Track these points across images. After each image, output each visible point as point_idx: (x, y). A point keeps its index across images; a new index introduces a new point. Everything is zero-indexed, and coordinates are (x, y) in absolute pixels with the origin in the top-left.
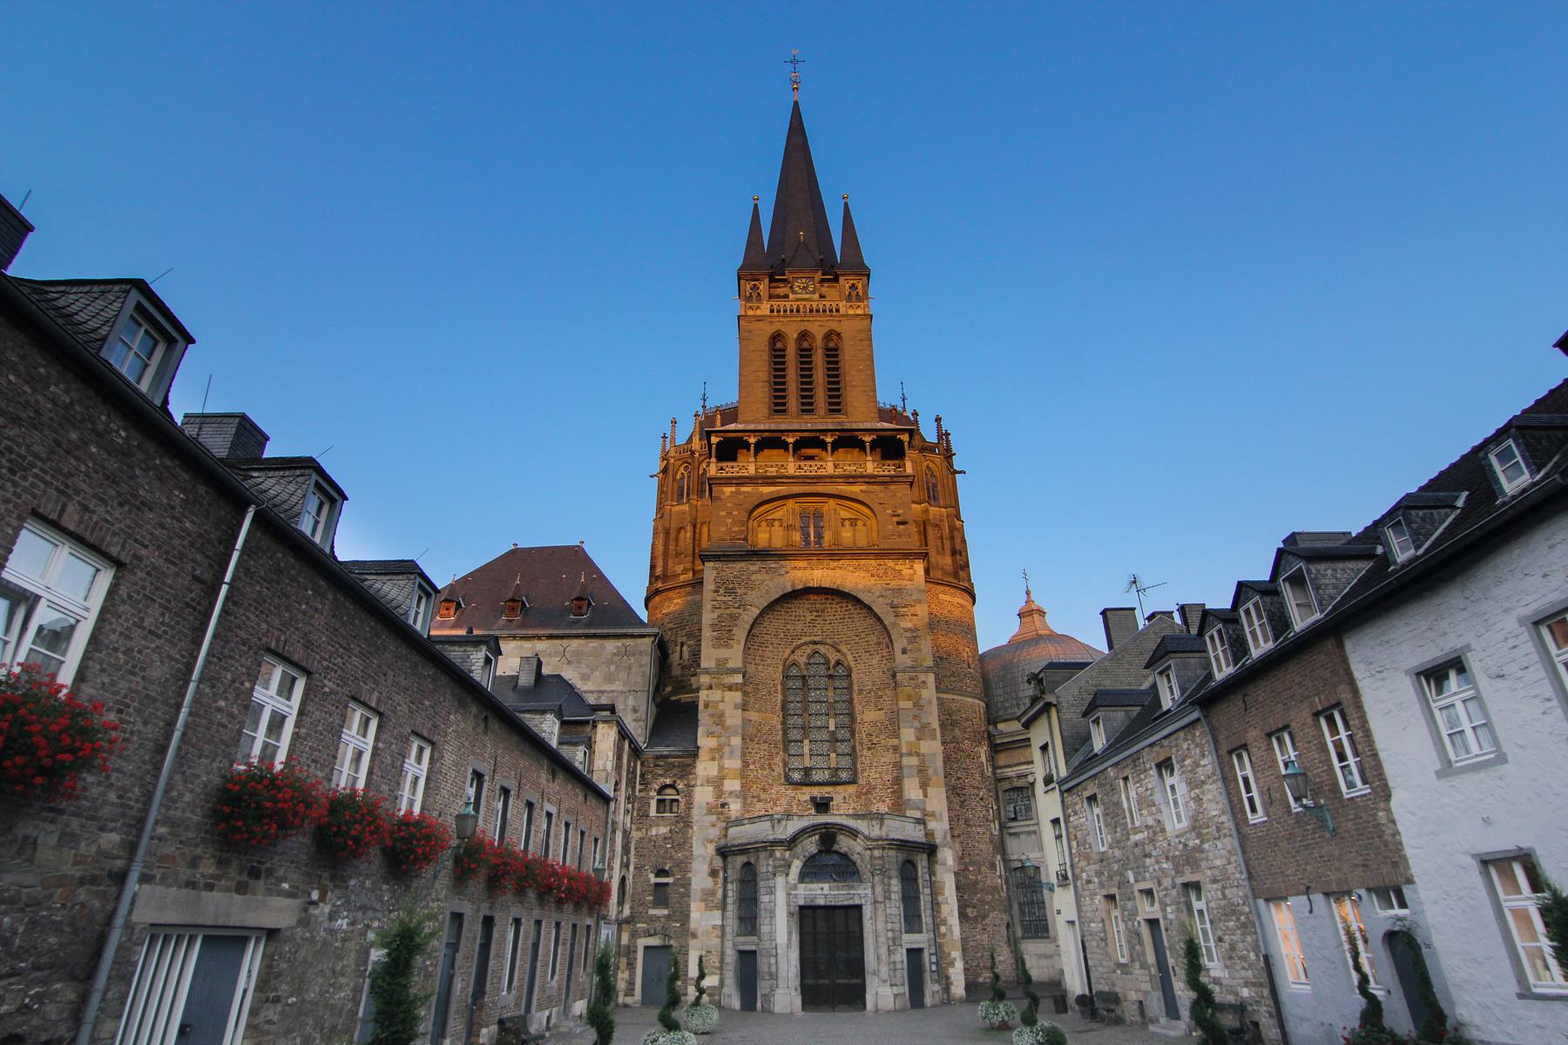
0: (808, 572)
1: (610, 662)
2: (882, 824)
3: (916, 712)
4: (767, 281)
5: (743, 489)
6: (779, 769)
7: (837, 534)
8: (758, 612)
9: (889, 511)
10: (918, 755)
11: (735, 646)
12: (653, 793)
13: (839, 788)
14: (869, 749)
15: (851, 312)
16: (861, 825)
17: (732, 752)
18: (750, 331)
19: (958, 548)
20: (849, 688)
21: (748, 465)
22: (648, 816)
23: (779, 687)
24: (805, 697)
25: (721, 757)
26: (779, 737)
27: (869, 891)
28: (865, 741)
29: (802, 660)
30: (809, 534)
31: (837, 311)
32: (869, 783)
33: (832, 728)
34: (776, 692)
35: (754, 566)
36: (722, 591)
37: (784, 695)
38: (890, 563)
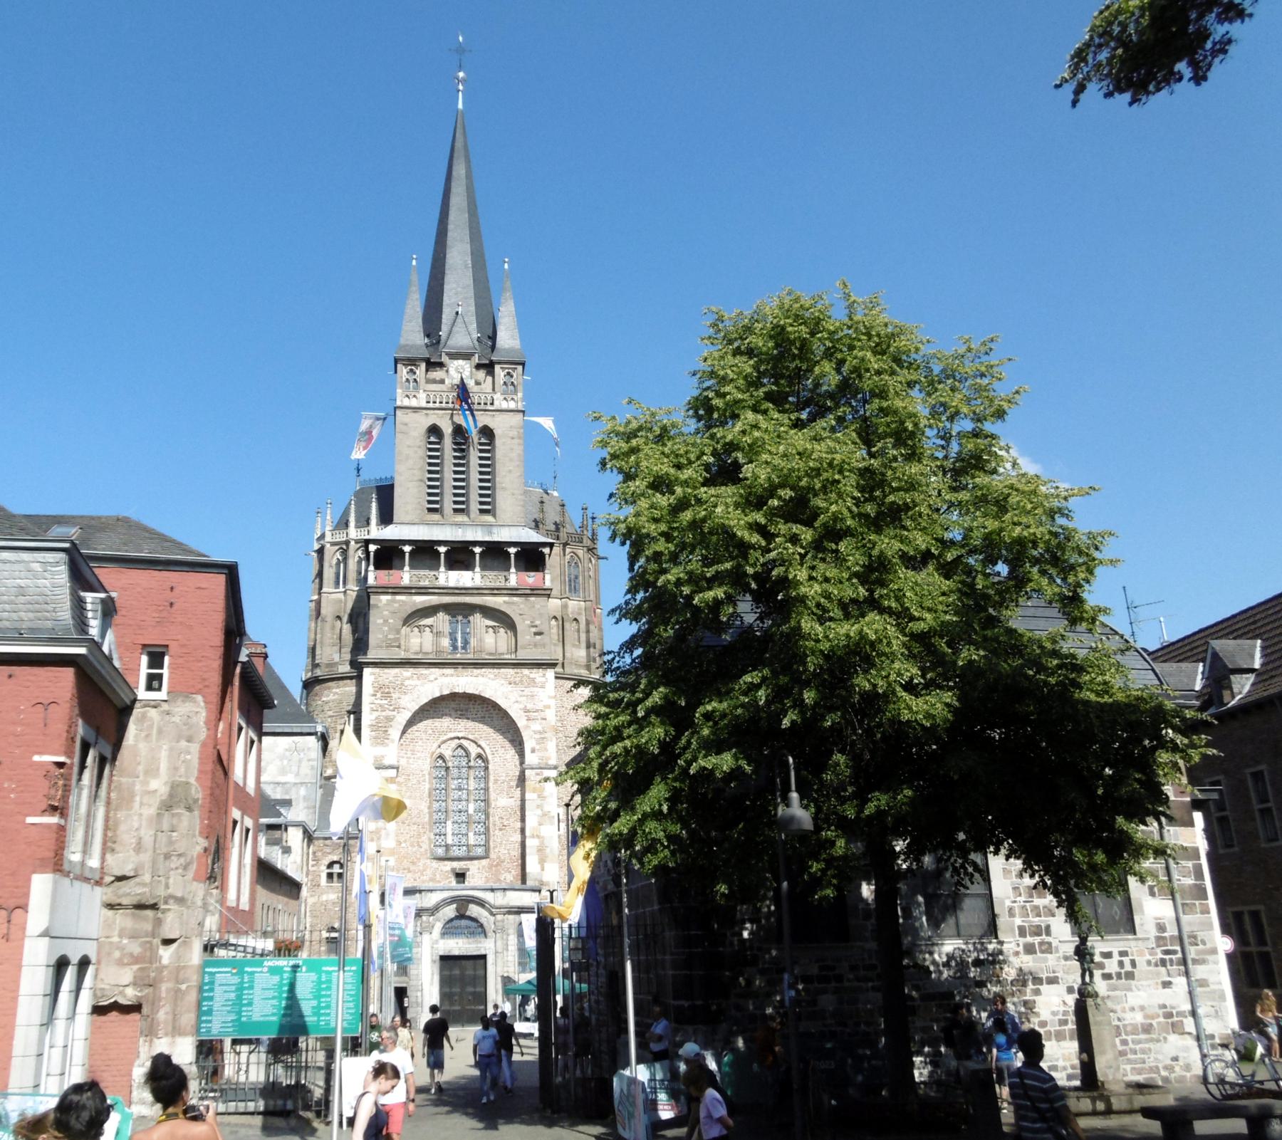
0: (454, 679)
1: (282, 758)
2: (505, 895)
3: (539, 802)
4: (423, 366)
5: (399, 597)
6: (425, 846)
7: (481, 640)
8: (408, 715)
9: (528, 622)
10: (538, 837)
11: (391, 744)
12: (323, 868)
13: (476, 862)
14: (501, 830)
15: (504, 405)
16: (488, 896)
17: (388, 835)
18: (406, 424)
19: (592, 641)
20: (486, 778)
21: (406, 576)
22: (319, 885)
23: (427, 777)
24: (447, 784)
25: (379, 839)
26: (427, 820)
27: (492, 945)
28: (498, 823)
29: (447, 753)
30: (456, 640)
31: (492, 404)
32: (499, 858)
33: (471, 811)
34: (424, 781)
35: (407, 672)
36: (379, 695)
37: (430, 783)
38: (526, 671)
